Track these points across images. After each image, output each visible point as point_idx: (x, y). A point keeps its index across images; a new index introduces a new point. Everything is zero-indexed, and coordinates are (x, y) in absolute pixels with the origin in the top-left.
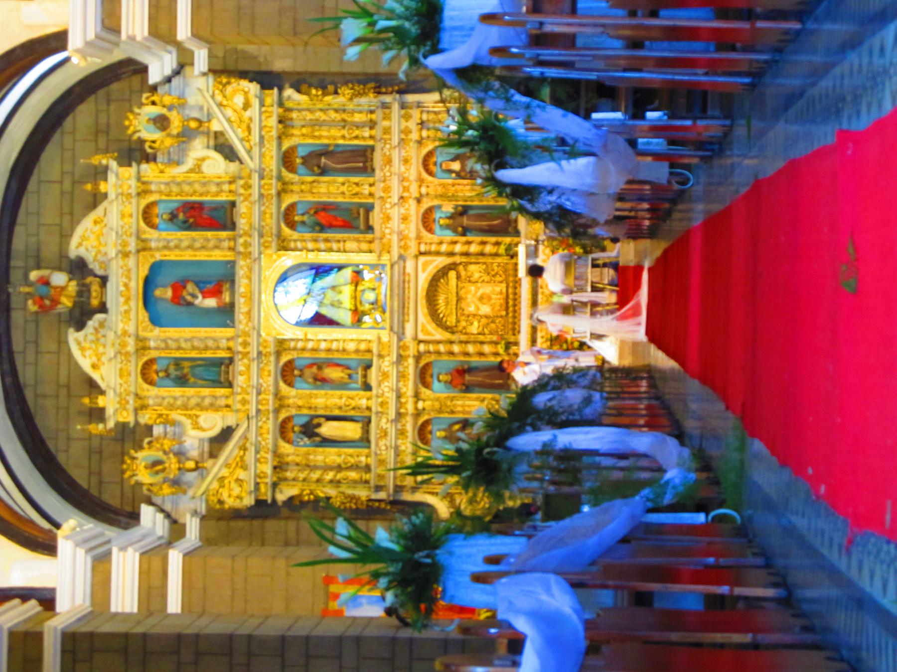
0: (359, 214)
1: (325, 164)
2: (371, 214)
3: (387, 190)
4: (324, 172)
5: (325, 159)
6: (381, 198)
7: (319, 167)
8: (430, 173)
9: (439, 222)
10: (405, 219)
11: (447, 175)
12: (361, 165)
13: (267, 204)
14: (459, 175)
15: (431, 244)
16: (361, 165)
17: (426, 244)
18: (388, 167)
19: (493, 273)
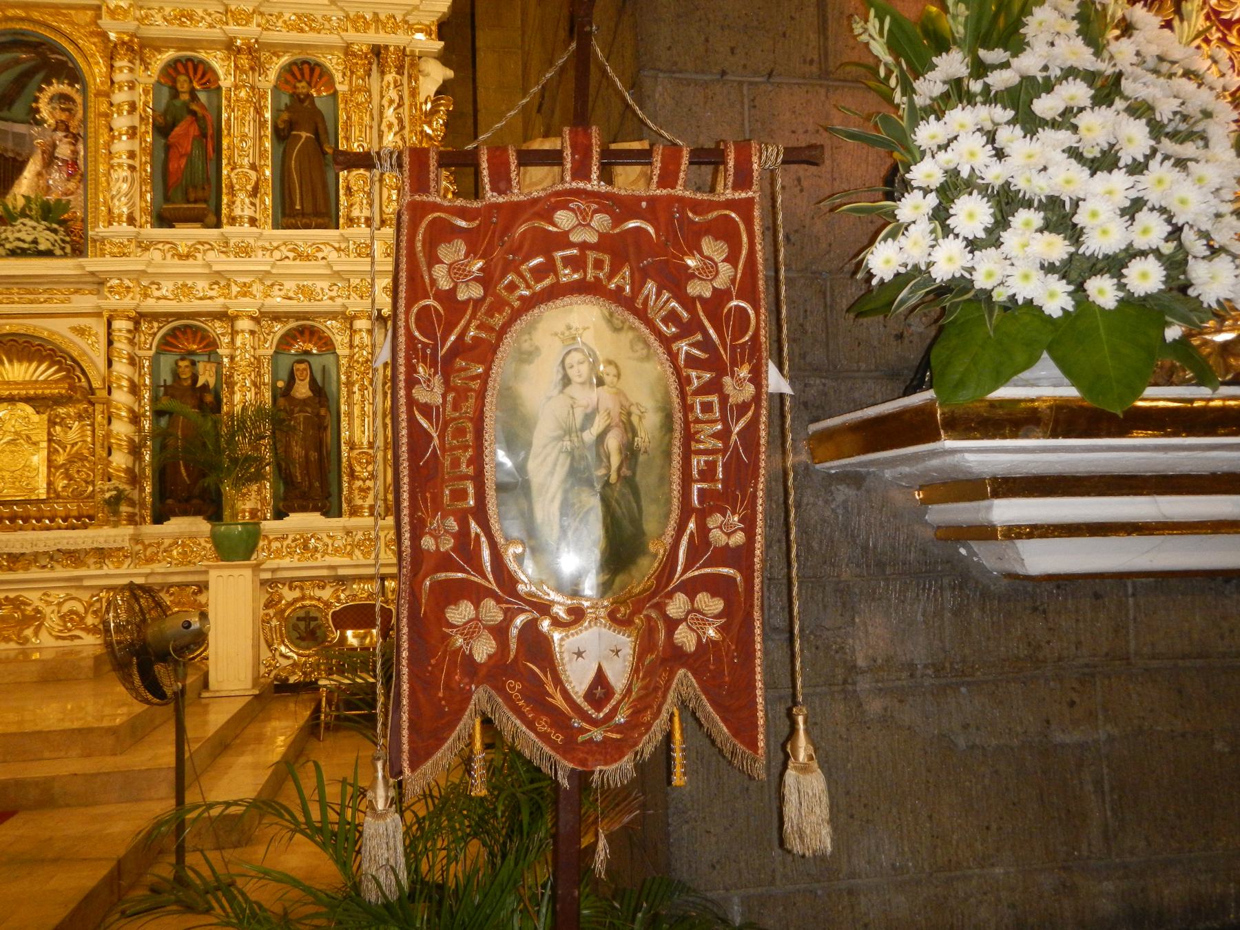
0: (196, 201)
1: (300, 137)
2: (199, 225)
3: (245, 251)
4: (282, 135)
5: (307, 137)
6: (227, 244)
7: (292, 125)
8: (287, 340)
9: (183, 359)
10: (185, 290)
11: (284, 374)
12: (298, 207)
13: (208, 19)
14: (284, 394)
15: (131, 342)
16: (298, 207)
17: (129, 331)
18: (291, 255)
19: (72, 471)
